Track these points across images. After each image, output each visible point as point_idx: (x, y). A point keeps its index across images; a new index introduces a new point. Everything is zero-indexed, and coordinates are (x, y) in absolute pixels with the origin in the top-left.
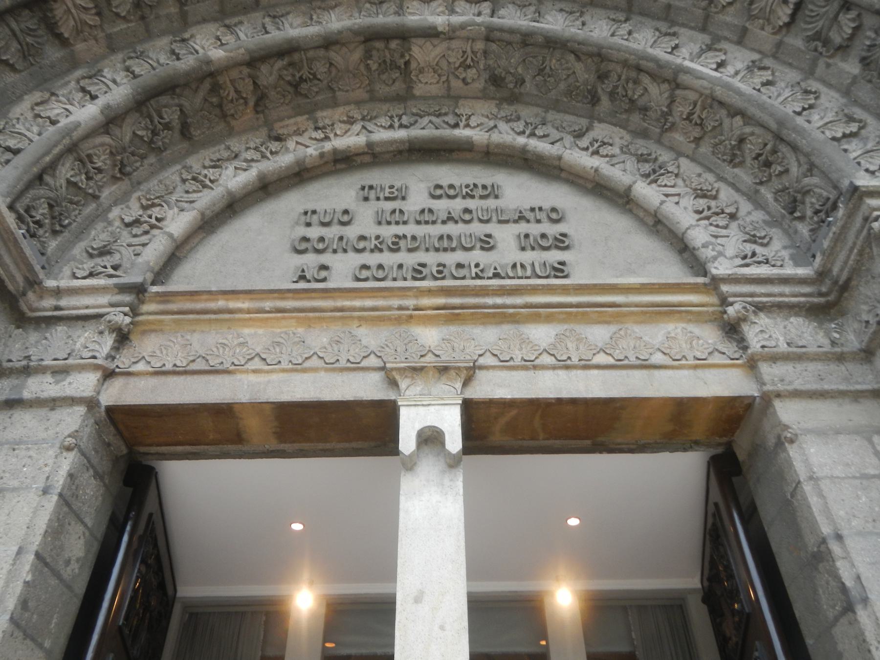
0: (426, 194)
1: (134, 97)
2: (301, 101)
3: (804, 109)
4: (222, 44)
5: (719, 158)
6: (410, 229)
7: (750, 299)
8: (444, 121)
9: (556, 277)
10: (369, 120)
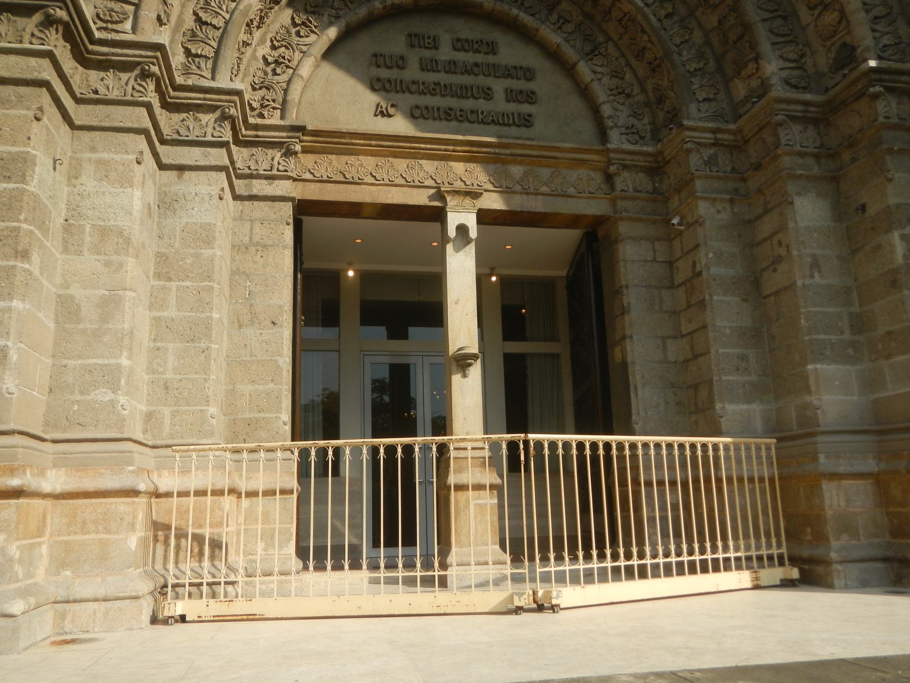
3: (682, 42)
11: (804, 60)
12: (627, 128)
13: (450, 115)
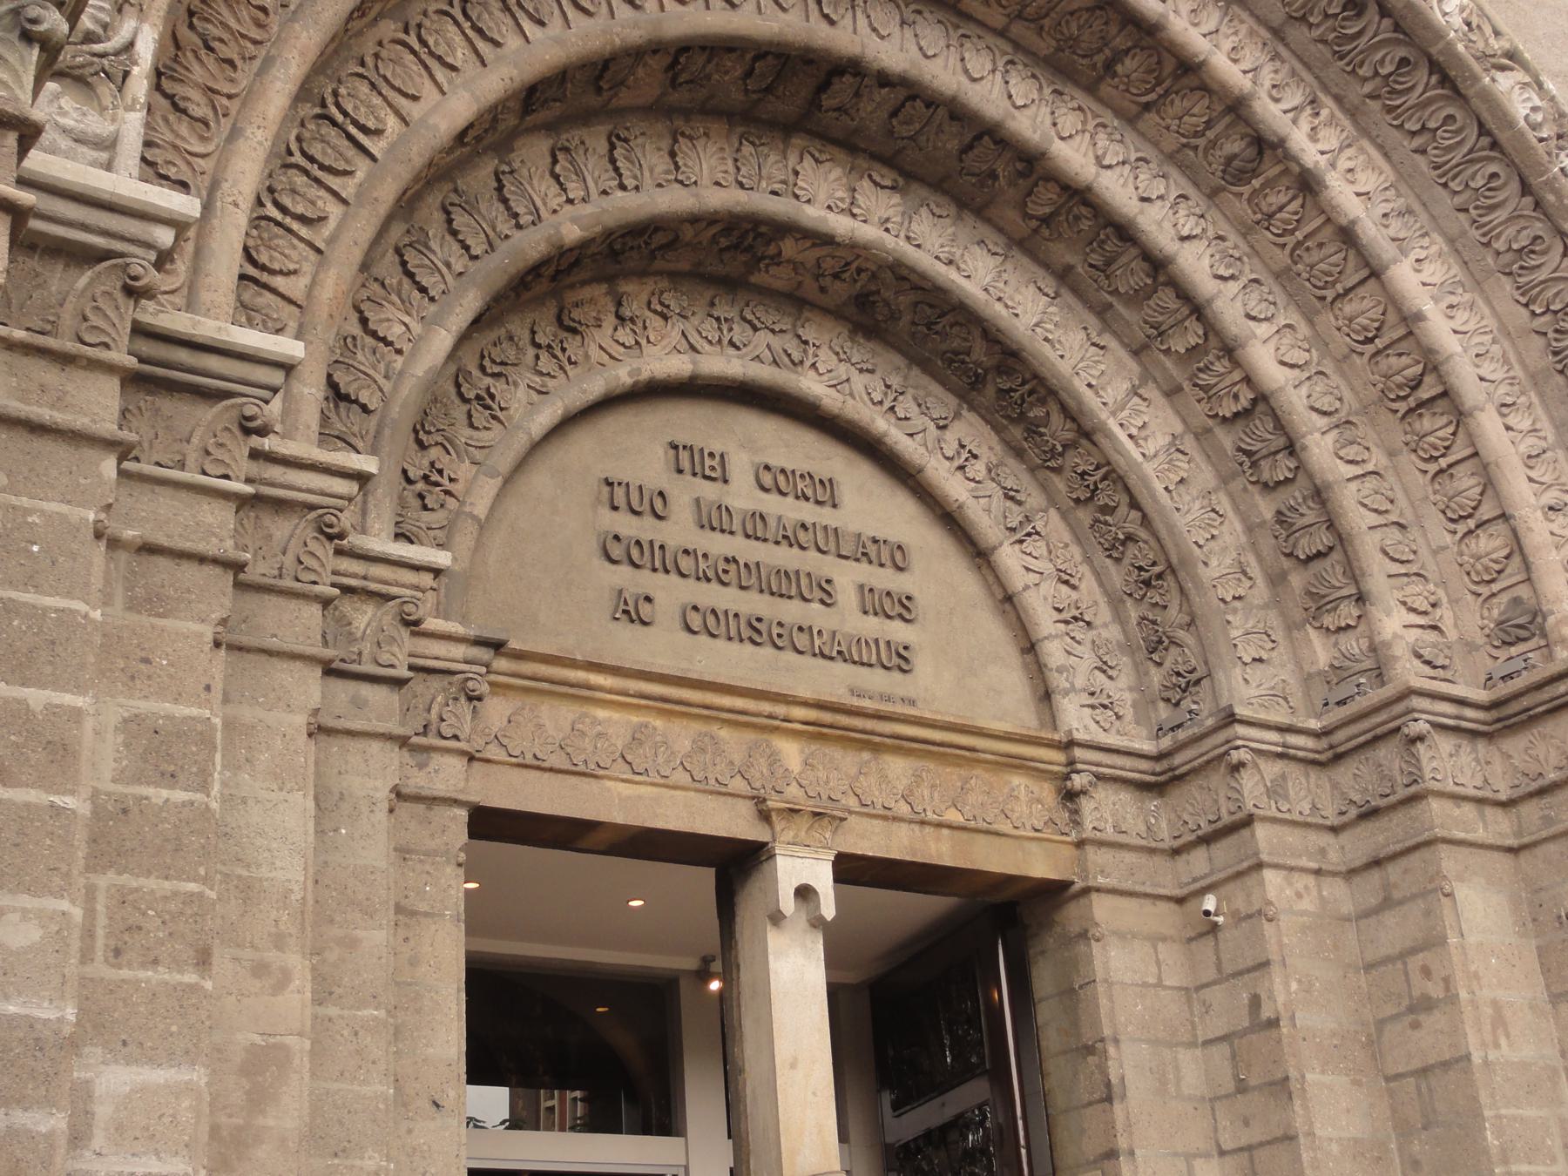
0: (752, 479)
7: (1094, 769)
11: (1438, 612)
12: (1092, 694)
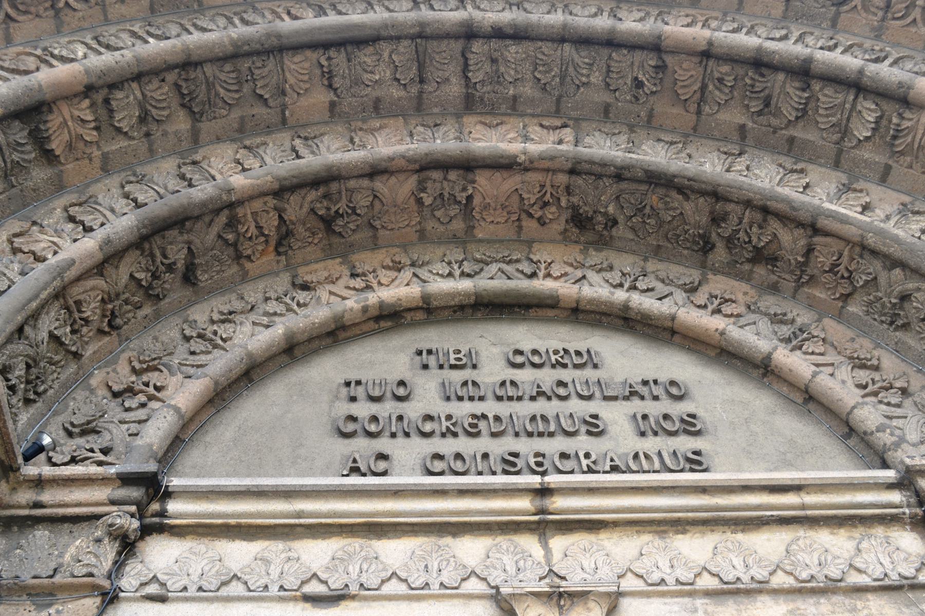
0: (503, 363)
1: (139, 230)
2: (336, 240)
4: (244, 170)
5: (875, 319)
6: (490, 407)
8: (518, 270)
9: (692, 470)
10: (420, 266)
13: (514, 465)
